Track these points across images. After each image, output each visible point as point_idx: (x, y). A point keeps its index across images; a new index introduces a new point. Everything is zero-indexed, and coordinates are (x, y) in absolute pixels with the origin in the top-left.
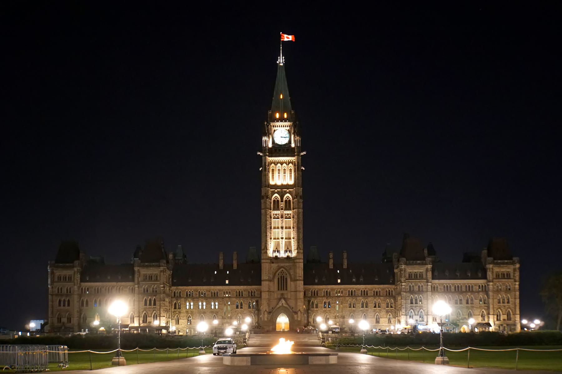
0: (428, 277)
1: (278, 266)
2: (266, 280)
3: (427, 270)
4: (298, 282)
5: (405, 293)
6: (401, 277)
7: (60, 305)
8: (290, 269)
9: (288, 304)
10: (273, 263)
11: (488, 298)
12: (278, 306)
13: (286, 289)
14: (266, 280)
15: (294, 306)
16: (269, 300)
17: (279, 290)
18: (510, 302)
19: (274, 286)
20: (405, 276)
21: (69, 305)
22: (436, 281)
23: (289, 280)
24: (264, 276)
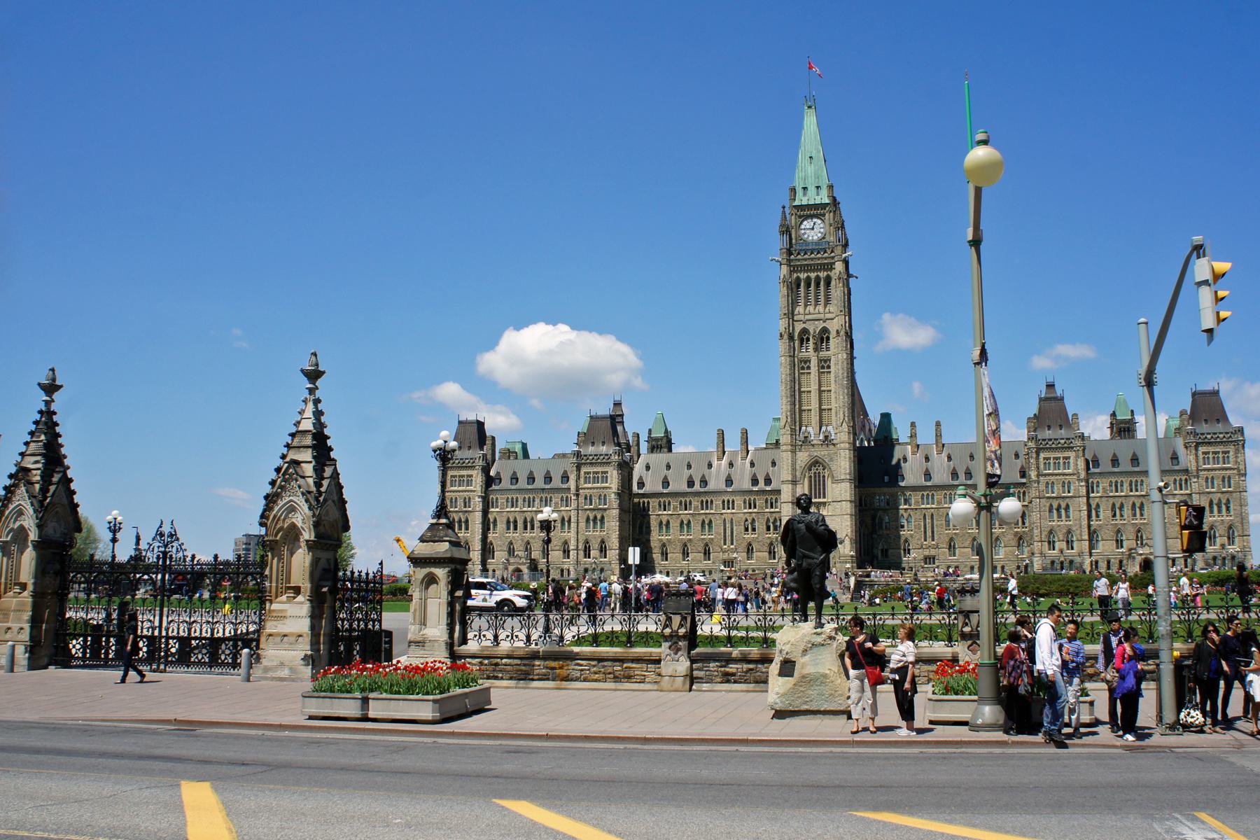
8: (831, 460)
21: (467, 529)
23: (829, 482)
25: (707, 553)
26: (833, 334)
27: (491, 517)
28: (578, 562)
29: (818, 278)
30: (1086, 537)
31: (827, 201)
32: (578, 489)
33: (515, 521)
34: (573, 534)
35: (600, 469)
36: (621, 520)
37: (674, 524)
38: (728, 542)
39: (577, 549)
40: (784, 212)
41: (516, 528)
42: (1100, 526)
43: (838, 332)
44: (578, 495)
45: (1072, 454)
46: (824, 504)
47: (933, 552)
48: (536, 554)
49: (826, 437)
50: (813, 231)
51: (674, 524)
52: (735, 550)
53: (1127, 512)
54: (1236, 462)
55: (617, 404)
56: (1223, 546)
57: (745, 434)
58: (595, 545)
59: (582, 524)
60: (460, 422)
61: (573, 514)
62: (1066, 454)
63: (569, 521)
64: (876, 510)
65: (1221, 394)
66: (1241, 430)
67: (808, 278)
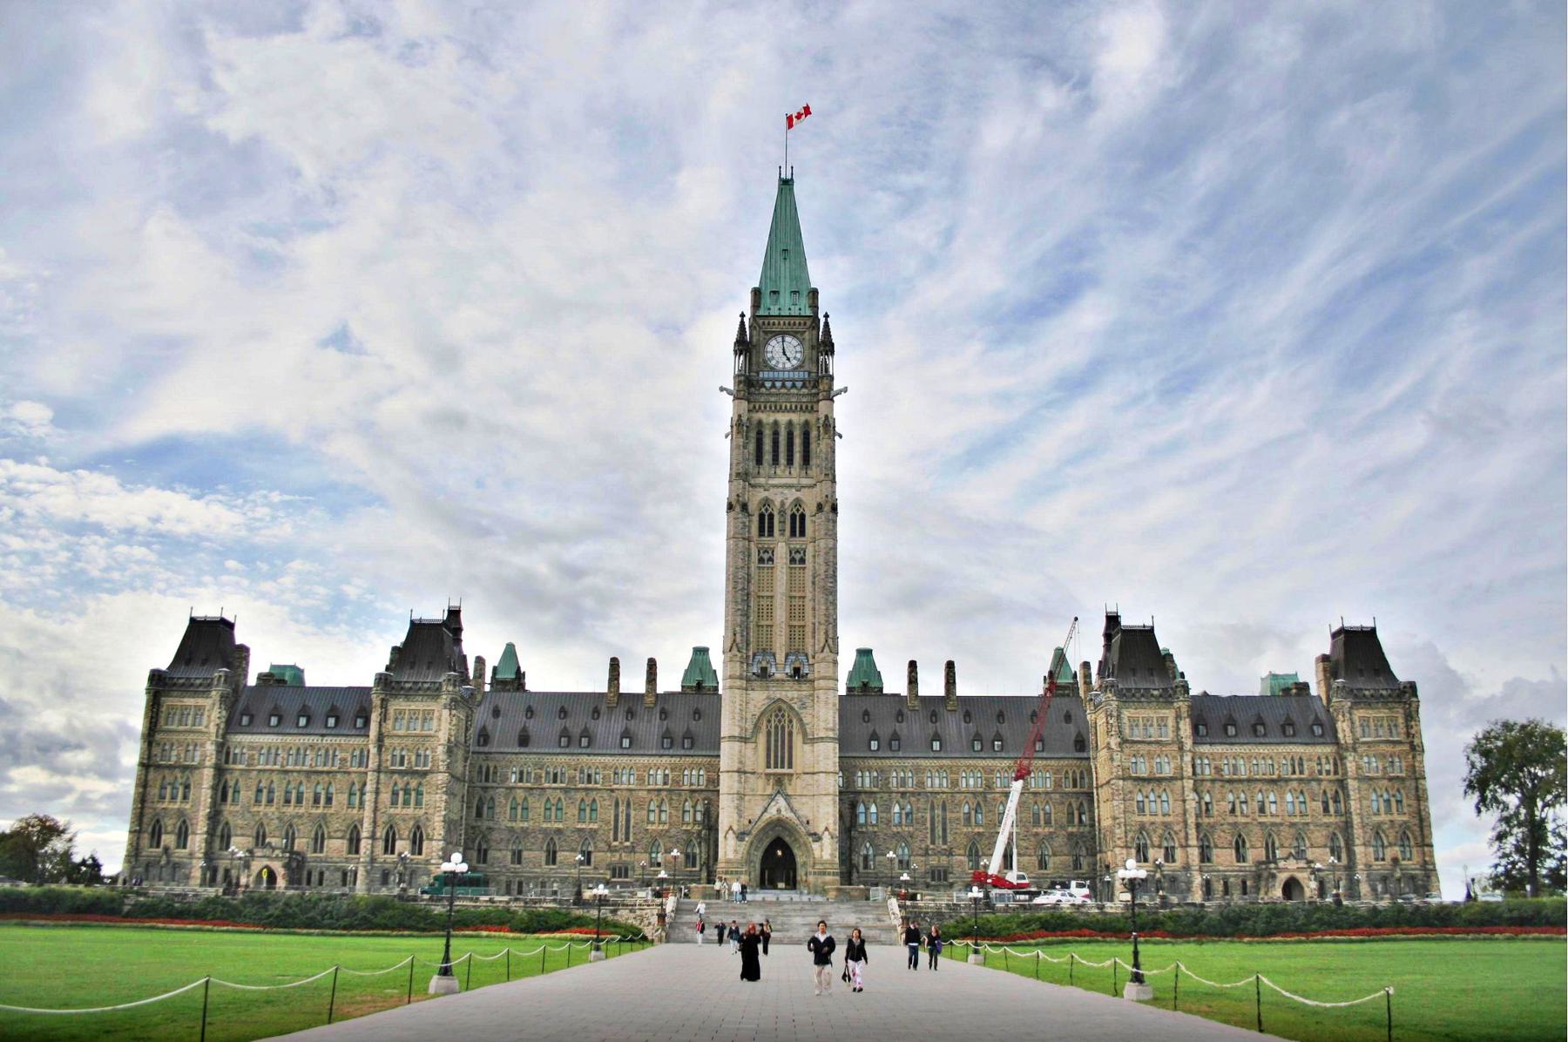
0: (1182, 733)
2: (732, 738)
3: (1178, 717)
4: (820, 746)
7: (162, 798)
8: (803, 706)
9: (792, 810)
11: (1347, 797)
12: (766, 816)
13: (790, 766)
14: (732, 738)
16: (741, 796)
19: (755, 755)
21: (185, 797)
22: (1205, 749)
23: (797, 739)
24: (728, 726)
28: (373, 860)
29: (790, 423)
30: (1193, 841)
31: (809, 312)
33: (271, 791)
35: (418, 705)
36: (450, 793)
38: (621, 836)
39: (373, 837)
40: (742, 323)
41: (270, 801)
42: (1213, 826)
43: (820, 507)
45: (1169, 714)
47: (944, 860)
48: (301, 844)
49: (797, 671)
51: (537, 804)
52: (632, 850)
53: (1256, 806)
54: (1408, 734)
55: (454, 614)
56: (1395, 861)
57: (652, 665)
59: (385, 797)
60: (192, 620)
61: (371, 777)
63: (362, 794)
65: (1380, 635)
66: (1412, 688)
67: (776, 423)
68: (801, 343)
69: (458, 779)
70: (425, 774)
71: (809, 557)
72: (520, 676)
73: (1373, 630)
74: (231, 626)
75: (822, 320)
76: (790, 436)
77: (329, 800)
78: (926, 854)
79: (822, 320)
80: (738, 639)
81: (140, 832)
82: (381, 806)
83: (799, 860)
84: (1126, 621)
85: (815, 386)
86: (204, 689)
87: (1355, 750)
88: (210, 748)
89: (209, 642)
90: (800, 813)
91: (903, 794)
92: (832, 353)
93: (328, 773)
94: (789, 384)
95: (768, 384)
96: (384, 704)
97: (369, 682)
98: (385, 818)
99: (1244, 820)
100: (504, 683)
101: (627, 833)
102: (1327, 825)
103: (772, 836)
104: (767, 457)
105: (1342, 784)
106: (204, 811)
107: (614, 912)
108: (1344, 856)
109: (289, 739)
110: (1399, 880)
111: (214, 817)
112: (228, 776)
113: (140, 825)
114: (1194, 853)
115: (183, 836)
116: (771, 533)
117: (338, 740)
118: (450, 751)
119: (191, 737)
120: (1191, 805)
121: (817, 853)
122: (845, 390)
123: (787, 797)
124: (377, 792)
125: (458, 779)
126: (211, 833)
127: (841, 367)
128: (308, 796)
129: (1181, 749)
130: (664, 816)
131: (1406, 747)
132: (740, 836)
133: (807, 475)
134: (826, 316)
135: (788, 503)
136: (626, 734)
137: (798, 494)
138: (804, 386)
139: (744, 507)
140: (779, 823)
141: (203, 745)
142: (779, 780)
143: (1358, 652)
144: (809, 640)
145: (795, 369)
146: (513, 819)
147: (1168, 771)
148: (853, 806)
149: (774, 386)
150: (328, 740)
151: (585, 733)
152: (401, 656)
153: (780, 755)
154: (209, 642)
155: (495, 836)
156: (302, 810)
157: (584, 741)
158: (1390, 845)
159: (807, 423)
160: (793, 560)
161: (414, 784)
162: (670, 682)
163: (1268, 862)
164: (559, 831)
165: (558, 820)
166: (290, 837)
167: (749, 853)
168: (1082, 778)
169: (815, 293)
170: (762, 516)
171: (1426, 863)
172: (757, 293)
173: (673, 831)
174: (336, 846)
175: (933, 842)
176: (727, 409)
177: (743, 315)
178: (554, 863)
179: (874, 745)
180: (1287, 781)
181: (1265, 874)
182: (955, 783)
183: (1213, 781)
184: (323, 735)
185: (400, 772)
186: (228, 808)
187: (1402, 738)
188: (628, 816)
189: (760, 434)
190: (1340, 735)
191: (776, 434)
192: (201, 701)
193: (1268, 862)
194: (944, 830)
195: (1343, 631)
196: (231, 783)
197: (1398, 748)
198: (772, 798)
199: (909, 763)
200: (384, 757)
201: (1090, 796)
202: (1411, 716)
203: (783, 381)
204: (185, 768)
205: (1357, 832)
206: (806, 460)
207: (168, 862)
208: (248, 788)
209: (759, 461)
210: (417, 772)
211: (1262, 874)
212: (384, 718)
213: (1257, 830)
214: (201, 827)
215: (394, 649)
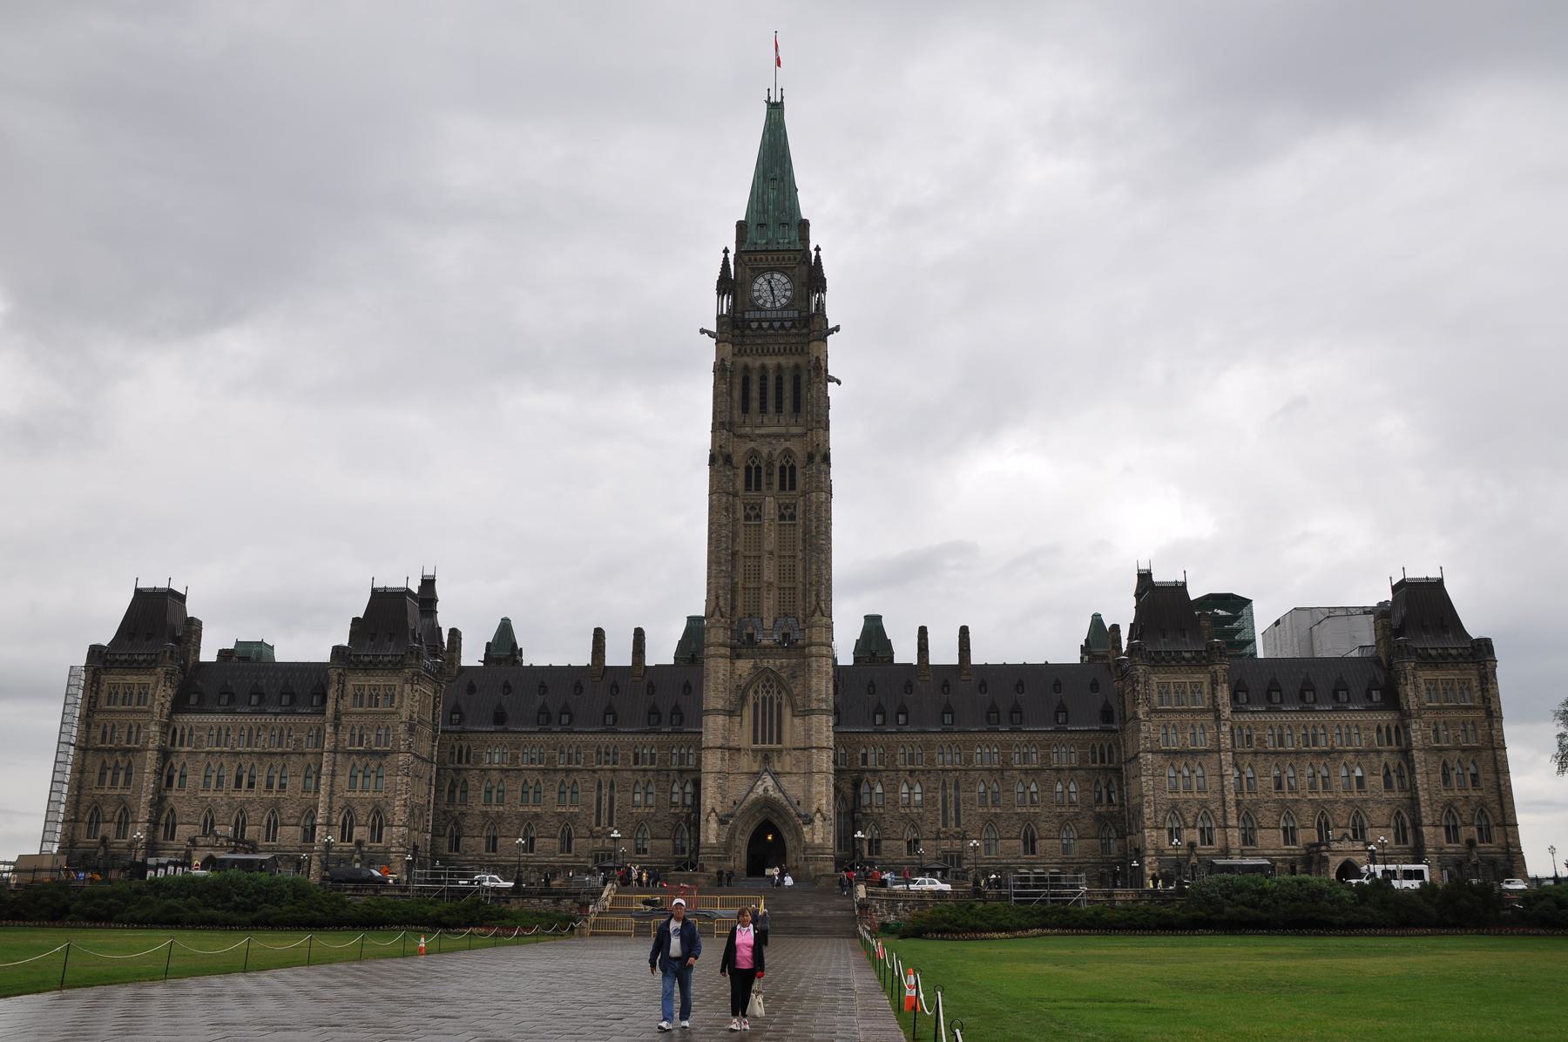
1: (755, 667)
3: (1214, 683)
4: (814, 718)
5: (1150, 756)
6: (1135, 703)
7: (101, 781)
10: (739, 657)
11: (1412, 771)
12: (753, 796)
13: (779, 741)
14: (717, 712)
15: (801, 796)
17: (755, 742)
18: (1483, 785)
20: (1148, 700)
21: (127, 782)
22: (1246, 718)
23: (787, 712)
24: (714, 697)
25: (567, 845)
26: (800, 459)
27: (177, 763)
29: (779, 367)
30: (1233, 822)
32: (337, 717)
34: (323, 796)
35: (379, 680)
37: (514, 787)
39: (329, 824)
41: (219, 783)
42: (1256, 803)
43: (811, 457)
44: (336, 727)
45: (1204, 678)
46: (780, 751)
48: (251, 832)
49: (786, 636)
50: (773, 291)
54: (1484, 698)
55: (428, 584)
56: (1471, 843)
57: (639, 635)
58: (362, 814)
59: (343, 780)
60: (138, 591)
62: (1196, 677)
63: (319, 778)
64: (864, 771)
65: (1449, 586)
67: (763, 367)
68: (791, 279)
69: (423, 760)
70: (385, 754)
71: (799, 513)
72: (516, 652)
73: (1439, 583)
74: (182, 598)
75: (814, 254)
76: (779, 379)
77: (282, 786)
78: (938, 838)
79: (814, 254)
80: (721, 603)
81: (76, 821)
82: (337, 789)
83: (790, 844)
84: (1157, 578)
85: (806, 326)
86: (149, 666)
87: (1419, 717)
88: (154, 728)
89: (157, 619)
90: (790, 793)
91: (912, 772)
92: (824, 290)
93: (282, 754)
94: (777, 325)
95: (754, 325)
96: (342, 683)
97: (327, 659)
98: (342, 803)
99: (1290, 797)
100: (499, 661)
101: (611, 818)
102: (1389, 802)
103: (760, 818)
104: (755, 405)
105: (1406, 753)
106: (146, 797)
107: (557, 902)
108: (1410, 838)
109: (240, 718)
110: (1476, 866)
111: (158, 803)
112: (174, 760)
113: (76, 814)
114: (1235, 836)
115: (124, 822)
116: (758, 488)
117: (293, 719)
118: (411, 729)
119: (131, 717)
120: (1230, 781)
121: (808, 838)
122: (837, 329)
123: (776, 775)
124: (333, 775)
125: (423, 760)
126: (154, 823)
127: (836, 305)
128: (261, 780)
129: (1218, 718)
130: (651, 800)
131: (1482, 714)
132: (722, 821)
133: (797, 424)
134: (818, 249)
135: (776, 454)
136: (610, 710)
137: (788, 444)
138: (793, 326)
139: (728, 459)
140: (767, 803)
141: (146, 726)
142: (767, 758)
143: (1421, 608)
144: (799, 602)
145: (784, 308)
146: (488, 802)
147: (1204, 742)
148: (856, 785)
149: (760, 327)
150: (282, 719)
151: (565, 710)
152: (359, 627)
153: (768, 728)
154: (157, 619)
155: (468, 821)
156: (253, 795)
157: (565, 719)
158: (1465, 824)
159: (797, 366)
160: (782, 517)
161: (373, 765)
162: (661, 652)
163: (1320, 845)
164: (537, 815)
165: (537, 803)
166: (240, 826)
167: (732, 836)
168: (1110, 752)
169: (804, 226)
170: (748, 469)
171: (1508, 845)
172: (741, 226)
173: (660, 816)
174: (289, 835)
175: (945, 825)
176: (708, 351)
177: (726, 251)
178: (532, 851)
179: (879, 719)
180: (1341, 752)
181: (1316, 857)
182: (969, 760)
183: (1256, 753)
184: (276, 714)
185: (358, 753)
186: (173, 795)
187: (1477, 702)
188: (611, 799)
189: (746, 382)
190: (1403, 701)
191: (763, 378)
192: (145, 679)
193: (1320, 845)
194: (957, 812)
195: (1403, 583)
196: (178, 767)
197: (1472, 715)
198: (756, 776)
199: (918, 738)
200: (340, 737)
201: (1119, 770)
202: (1487, 679)
203: (771, 321)
204: (129, 750)
205: (1424, 810)
206: (797, 408)
207: (106, 853)
208: (196, 772)
209: (745, 408)
210: (376, 752)
211: (1313, 858)
212: (342, 694)
213: (1307, 810)
214: (143, 814)
215: (355, 620)
